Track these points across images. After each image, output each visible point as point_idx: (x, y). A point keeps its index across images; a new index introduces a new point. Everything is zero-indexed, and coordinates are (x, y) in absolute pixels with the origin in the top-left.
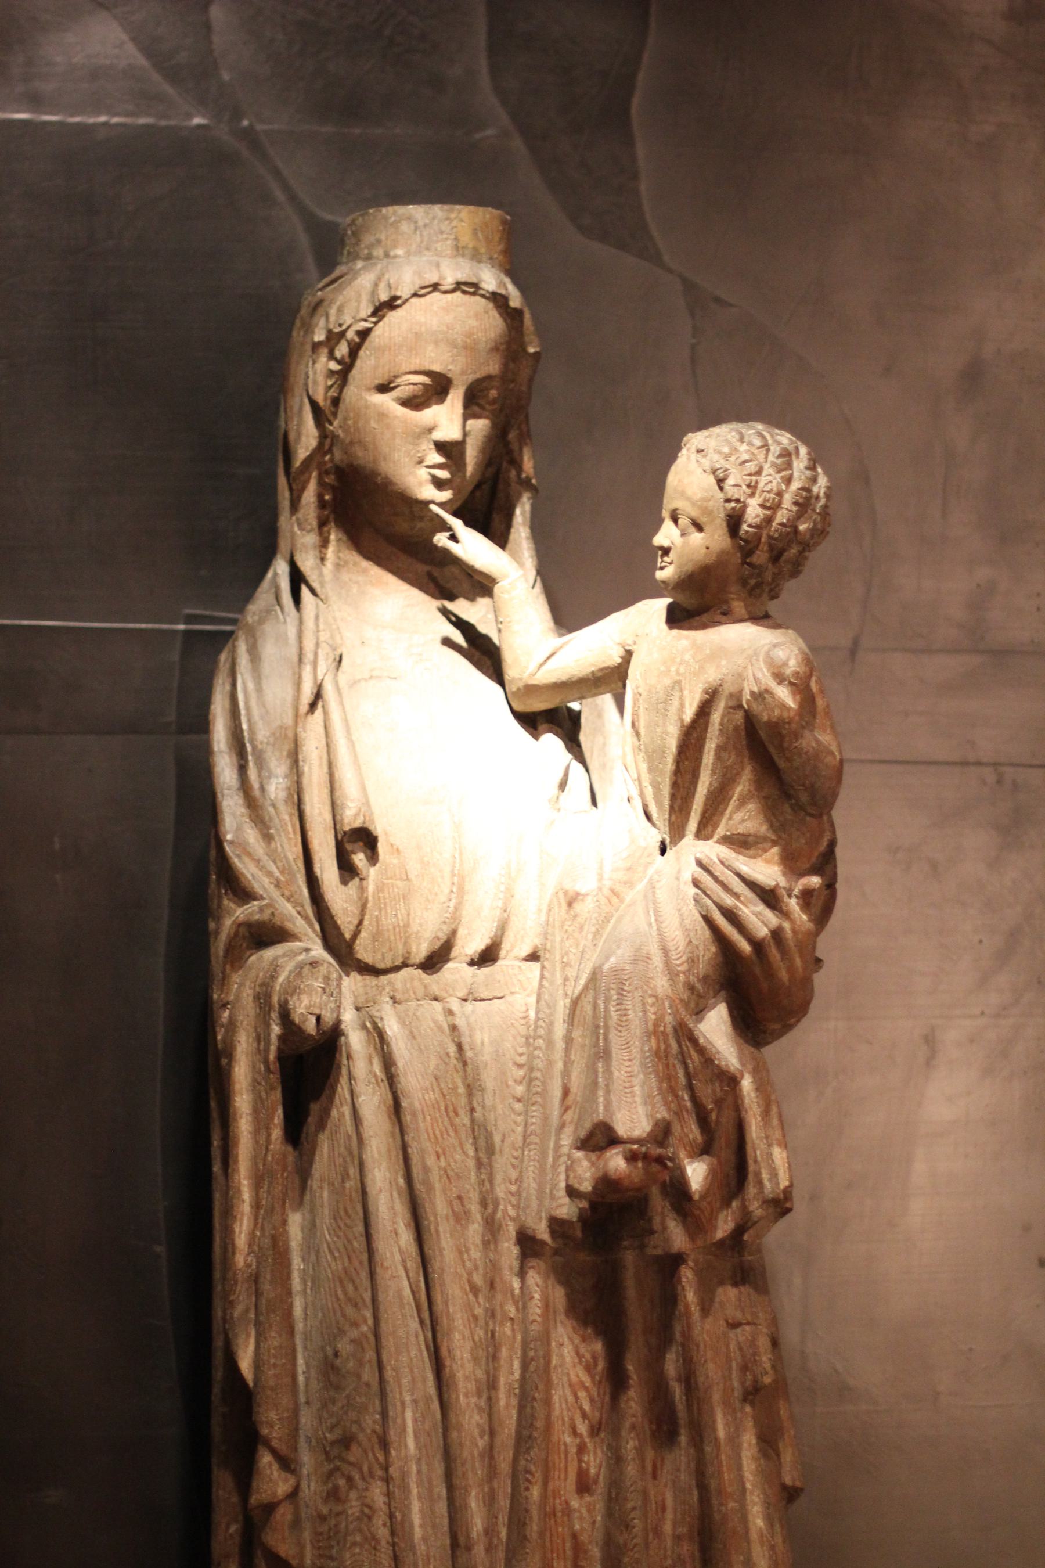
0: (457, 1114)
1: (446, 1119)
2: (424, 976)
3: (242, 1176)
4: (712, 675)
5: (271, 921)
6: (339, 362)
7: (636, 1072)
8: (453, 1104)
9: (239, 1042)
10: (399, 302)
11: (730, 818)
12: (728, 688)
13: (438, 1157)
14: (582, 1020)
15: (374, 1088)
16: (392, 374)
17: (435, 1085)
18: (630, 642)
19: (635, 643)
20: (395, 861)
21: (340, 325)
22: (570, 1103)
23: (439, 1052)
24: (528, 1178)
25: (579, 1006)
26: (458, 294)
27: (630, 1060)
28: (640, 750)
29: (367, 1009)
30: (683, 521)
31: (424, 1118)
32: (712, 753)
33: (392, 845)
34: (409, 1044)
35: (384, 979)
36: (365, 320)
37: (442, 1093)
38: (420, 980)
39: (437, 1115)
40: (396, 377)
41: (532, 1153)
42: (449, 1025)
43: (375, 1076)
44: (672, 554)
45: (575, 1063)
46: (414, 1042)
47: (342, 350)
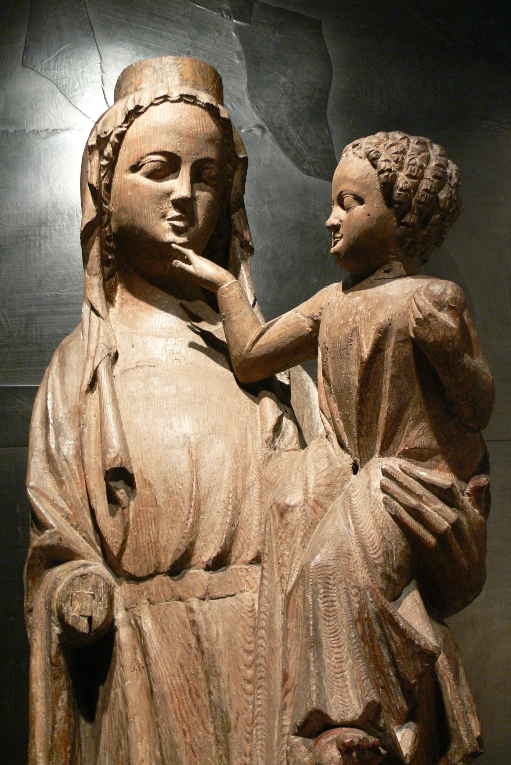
0: (198, 696)
1: (190, 700)
2: (171, 581)
3: (38, 750)
4: (382, 317)
5: (59, 544)
6: (107, 159)
7: (345, 658)
8: (195, 688)
9: (35, 640)
10: (141, 110)
11: (408, 436)
12: (397, 326)
13: (185, 734)
14: (295, 612)
15: (137, 674)
16: (139, 157)
17: (180, 671)
18: (316, 314)
19: (321, 314)
20: (148, 493)
21: (105, 133)
22: (289, 687)
23: (183, 644)
24: (257, 756)
25: (292, 600)
26: (182, 103)
27: (339, 647)
28: (331, 393)
29: (132, 610)
30: (348, 199)
31: (173, 700)
32: (388, 382)
33: (145, 480)
34: (160, 637)
35: (143, 585)
36: (121, 127)
37: (186, 678)
38: (169, 584)
39: (183, 697)
40: (142, 158)
41: (259, 732)
42: (190, 621)
43: (138, 663)
44: (341, 231)
45: (292, 650)
46: (164, 635)
47: (109, 150)
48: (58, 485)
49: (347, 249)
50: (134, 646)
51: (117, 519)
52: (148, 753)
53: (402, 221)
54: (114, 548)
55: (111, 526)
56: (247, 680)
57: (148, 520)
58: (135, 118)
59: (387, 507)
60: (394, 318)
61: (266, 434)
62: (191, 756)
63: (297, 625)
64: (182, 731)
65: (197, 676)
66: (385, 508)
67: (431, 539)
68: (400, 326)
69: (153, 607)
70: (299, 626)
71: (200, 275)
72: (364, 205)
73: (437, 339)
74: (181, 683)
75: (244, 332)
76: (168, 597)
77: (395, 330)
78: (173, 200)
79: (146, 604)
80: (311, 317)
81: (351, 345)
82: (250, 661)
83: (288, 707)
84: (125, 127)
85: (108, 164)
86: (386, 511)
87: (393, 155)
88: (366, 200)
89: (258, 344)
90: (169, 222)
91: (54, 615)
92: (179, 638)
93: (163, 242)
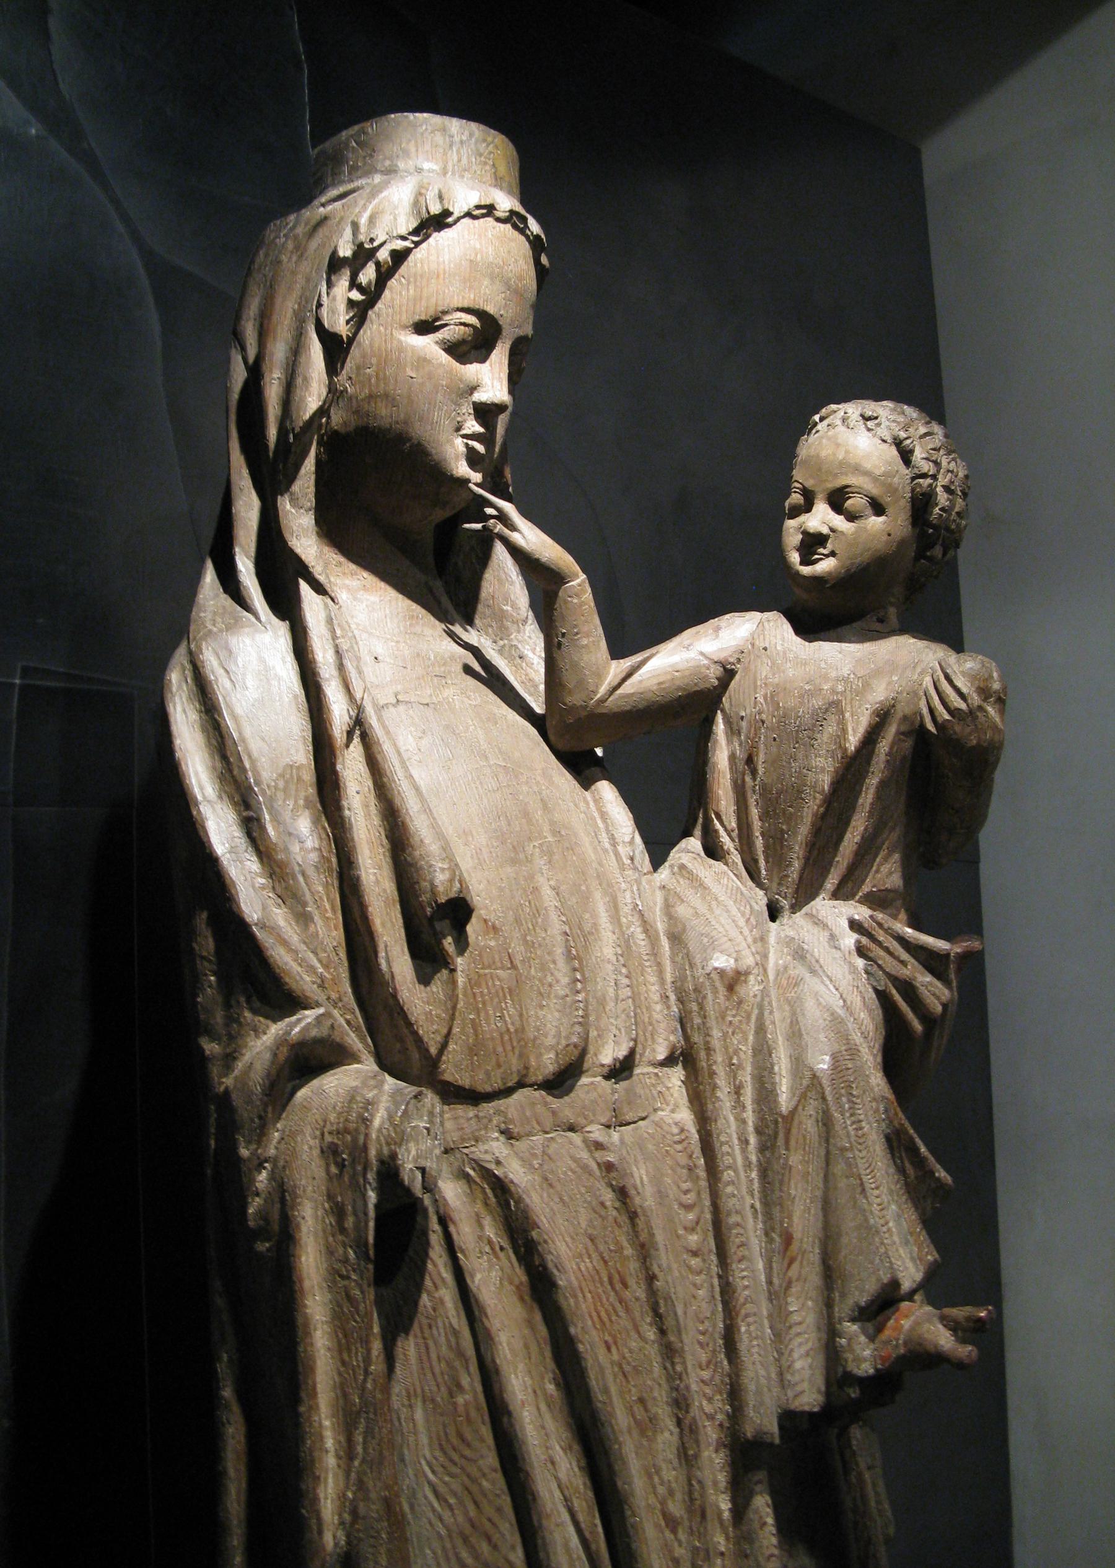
0: (625, 1285)
1: (612, 1294)
2: (550, 1098)
3: (323, 1416)
4: (879, 694)
5: (330, 1036)
6: (361, 289)
7: (886, 1204)
8: (619, 1273)
9: (303, 1218)
10: (450, 220)
11: (877, 871)
12: (902, 709)
13: (609, 1349)
14: (801, 1141)
15: (489, 1261)
16: (440, 309)
17: (591, 1248)
18: (731, 660)
19: (739, 660)
20: (492, 943)
21: (372, 240)
22: (794, 1254)
23: (589, 1203)
24: (754, 1363)
25: (796, 1122)
26: (509, 226)
27: (877, 1188)
28: (754, 791)
29: (465, 1151)
30: (854, 502)
31: (584, 1297)
32: (872, 791)
33: (485, 921)
34: (545, 1195)
35: (488, 1108)
36: (404, 238)
37: (603, 1258)
38: (546, 1104)
39: (600, 1291)
40: (445, 313)
41: (752, 1328)
42: (598, 1164)
43: (490, 1242)
44: (829, 546)
45: (797, 1199)
46: (551, 1190)
47: (368, 274)
48: (297, 922)
49: (843, 578)
50: (477, 1215)
51: (435, 990)
52: (530, 1390)
53: (928, 554)
54: (431, 1043)
55: (423, 1002)
56: (691, 1251)
57: (497, 992)
58: (435, 231)
59: (872, 979)
60: (900, 697)
61: (546, 837)
62: (621, 1382)
63: (804, 1160)
64: (604, 1345)
65: (622, 1253)
66: (868, 979)
67: (917, 1026)
68: (907, 711)
69: (517, 1143)
70: (808, 1162)
71: (537, 556)
72: (882, 519)
73: (982, 743)
74: (594, 1267)
75: (598, 668)
76: (548, 1126)
77: (899, 715)
78: (482, 404)
79: (497, 1139)
80: (722, 664)
81: (821, 725)
82: (691, 1221)
83: (793, 1285)
84: (413, 242)
85: (363, 300)
86: (869, 984)
87: (931, 452)
88: (890, 510)
89: (620, 691)
90: (465, 441)
91: (372, 1170)
92: (582, 1195)
93: (452, 475)
